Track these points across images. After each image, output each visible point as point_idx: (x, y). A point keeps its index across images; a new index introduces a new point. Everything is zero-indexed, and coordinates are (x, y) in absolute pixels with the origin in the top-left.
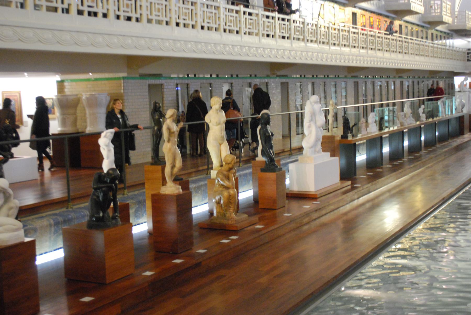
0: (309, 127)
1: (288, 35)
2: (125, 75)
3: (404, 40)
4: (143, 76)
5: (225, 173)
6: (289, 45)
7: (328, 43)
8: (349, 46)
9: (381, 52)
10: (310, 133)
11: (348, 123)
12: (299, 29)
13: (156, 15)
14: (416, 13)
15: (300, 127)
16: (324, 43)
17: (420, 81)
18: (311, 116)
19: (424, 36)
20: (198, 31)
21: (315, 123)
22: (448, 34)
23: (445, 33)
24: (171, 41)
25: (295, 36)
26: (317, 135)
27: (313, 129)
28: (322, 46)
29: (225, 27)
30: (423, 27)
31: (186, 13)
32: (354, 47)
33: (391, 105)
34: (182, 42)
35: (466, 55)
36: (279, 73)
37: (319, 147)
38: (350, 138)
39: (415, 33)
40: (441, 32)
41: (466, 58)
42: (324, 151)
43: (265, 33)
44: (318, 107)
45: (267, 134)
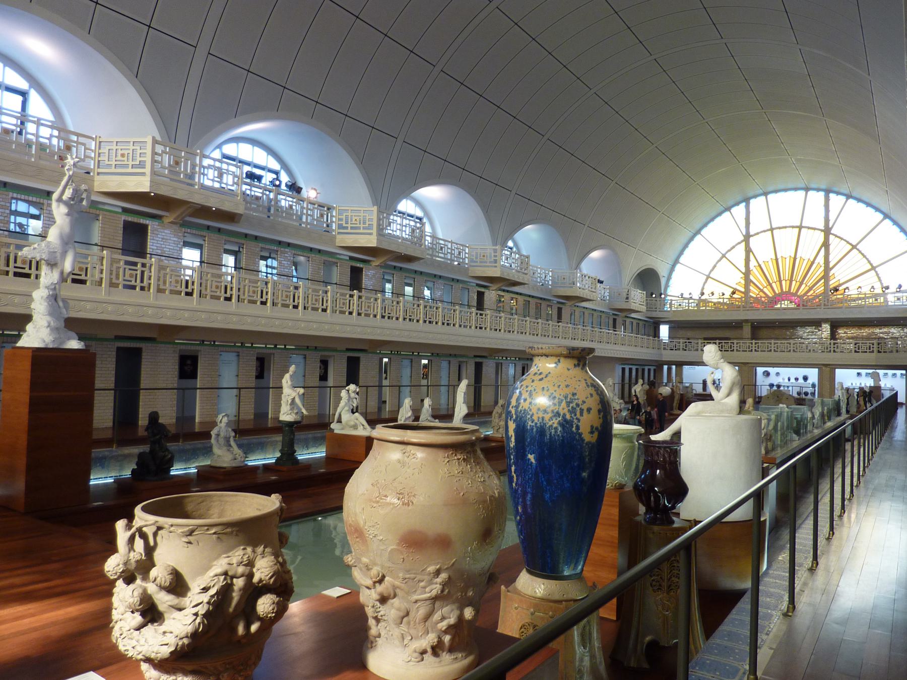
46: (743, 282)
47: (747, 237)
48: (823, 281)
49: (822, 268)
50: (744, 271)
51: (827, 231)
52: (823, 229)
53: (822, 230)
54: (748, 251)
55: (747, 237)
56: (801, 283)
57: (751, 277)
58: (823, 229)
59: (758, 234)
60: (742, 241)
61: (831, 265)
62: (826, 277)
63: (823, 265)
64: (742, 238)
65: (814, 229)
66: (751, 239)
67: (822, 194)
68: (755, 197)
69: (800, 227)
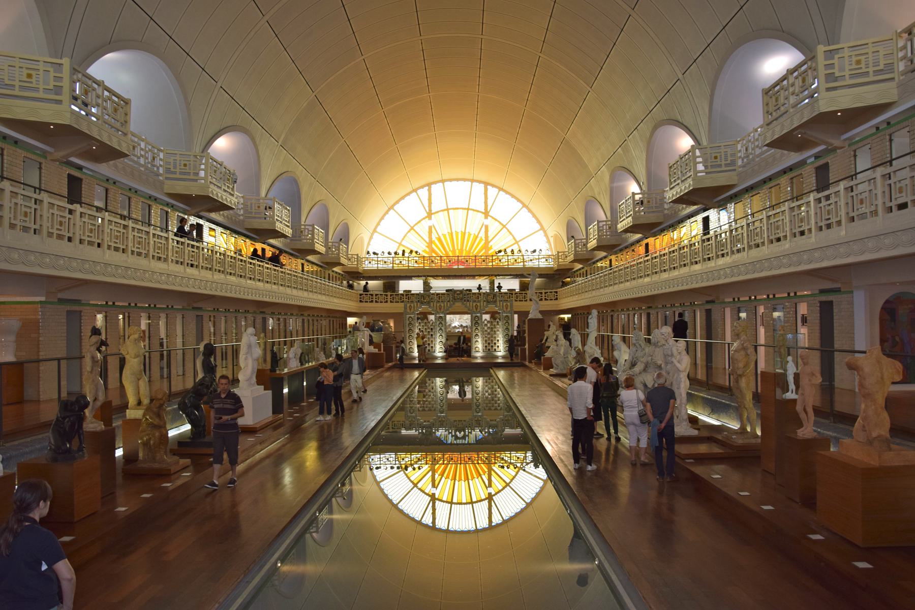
0: (246, 359)
1: (210, 266)
2: (43, 299)
3: (305, 277)
4: (61, 301)
5: (155, 410)
6: (211, 277)
8: (262, 281)
10: (246, 366)
11: (276, 357)
12: (220, 260)
13: (88, 236)
14: (319, 253)
15: (224, 361)
16: (241, 276)
17: (315, 319)
18: (248, 348)
19: (323, 276)
20: (128, 256)
21: (252, 356)
24: (102, 265)
25: (217, 268)
26: (253, 366)
29: (154, 254)
30: (321, 266)
31: (117, 236)
32: (267, 282)
33: (306, 341)
34: (113, 266)
36: (195, 305)
37: (254, 379)
38: (278, 372)
39: (319, 273)
42: (259, 383)
43: (190, 262)
44: (254, 339)
48: (484, 251)
62: (486, 246)
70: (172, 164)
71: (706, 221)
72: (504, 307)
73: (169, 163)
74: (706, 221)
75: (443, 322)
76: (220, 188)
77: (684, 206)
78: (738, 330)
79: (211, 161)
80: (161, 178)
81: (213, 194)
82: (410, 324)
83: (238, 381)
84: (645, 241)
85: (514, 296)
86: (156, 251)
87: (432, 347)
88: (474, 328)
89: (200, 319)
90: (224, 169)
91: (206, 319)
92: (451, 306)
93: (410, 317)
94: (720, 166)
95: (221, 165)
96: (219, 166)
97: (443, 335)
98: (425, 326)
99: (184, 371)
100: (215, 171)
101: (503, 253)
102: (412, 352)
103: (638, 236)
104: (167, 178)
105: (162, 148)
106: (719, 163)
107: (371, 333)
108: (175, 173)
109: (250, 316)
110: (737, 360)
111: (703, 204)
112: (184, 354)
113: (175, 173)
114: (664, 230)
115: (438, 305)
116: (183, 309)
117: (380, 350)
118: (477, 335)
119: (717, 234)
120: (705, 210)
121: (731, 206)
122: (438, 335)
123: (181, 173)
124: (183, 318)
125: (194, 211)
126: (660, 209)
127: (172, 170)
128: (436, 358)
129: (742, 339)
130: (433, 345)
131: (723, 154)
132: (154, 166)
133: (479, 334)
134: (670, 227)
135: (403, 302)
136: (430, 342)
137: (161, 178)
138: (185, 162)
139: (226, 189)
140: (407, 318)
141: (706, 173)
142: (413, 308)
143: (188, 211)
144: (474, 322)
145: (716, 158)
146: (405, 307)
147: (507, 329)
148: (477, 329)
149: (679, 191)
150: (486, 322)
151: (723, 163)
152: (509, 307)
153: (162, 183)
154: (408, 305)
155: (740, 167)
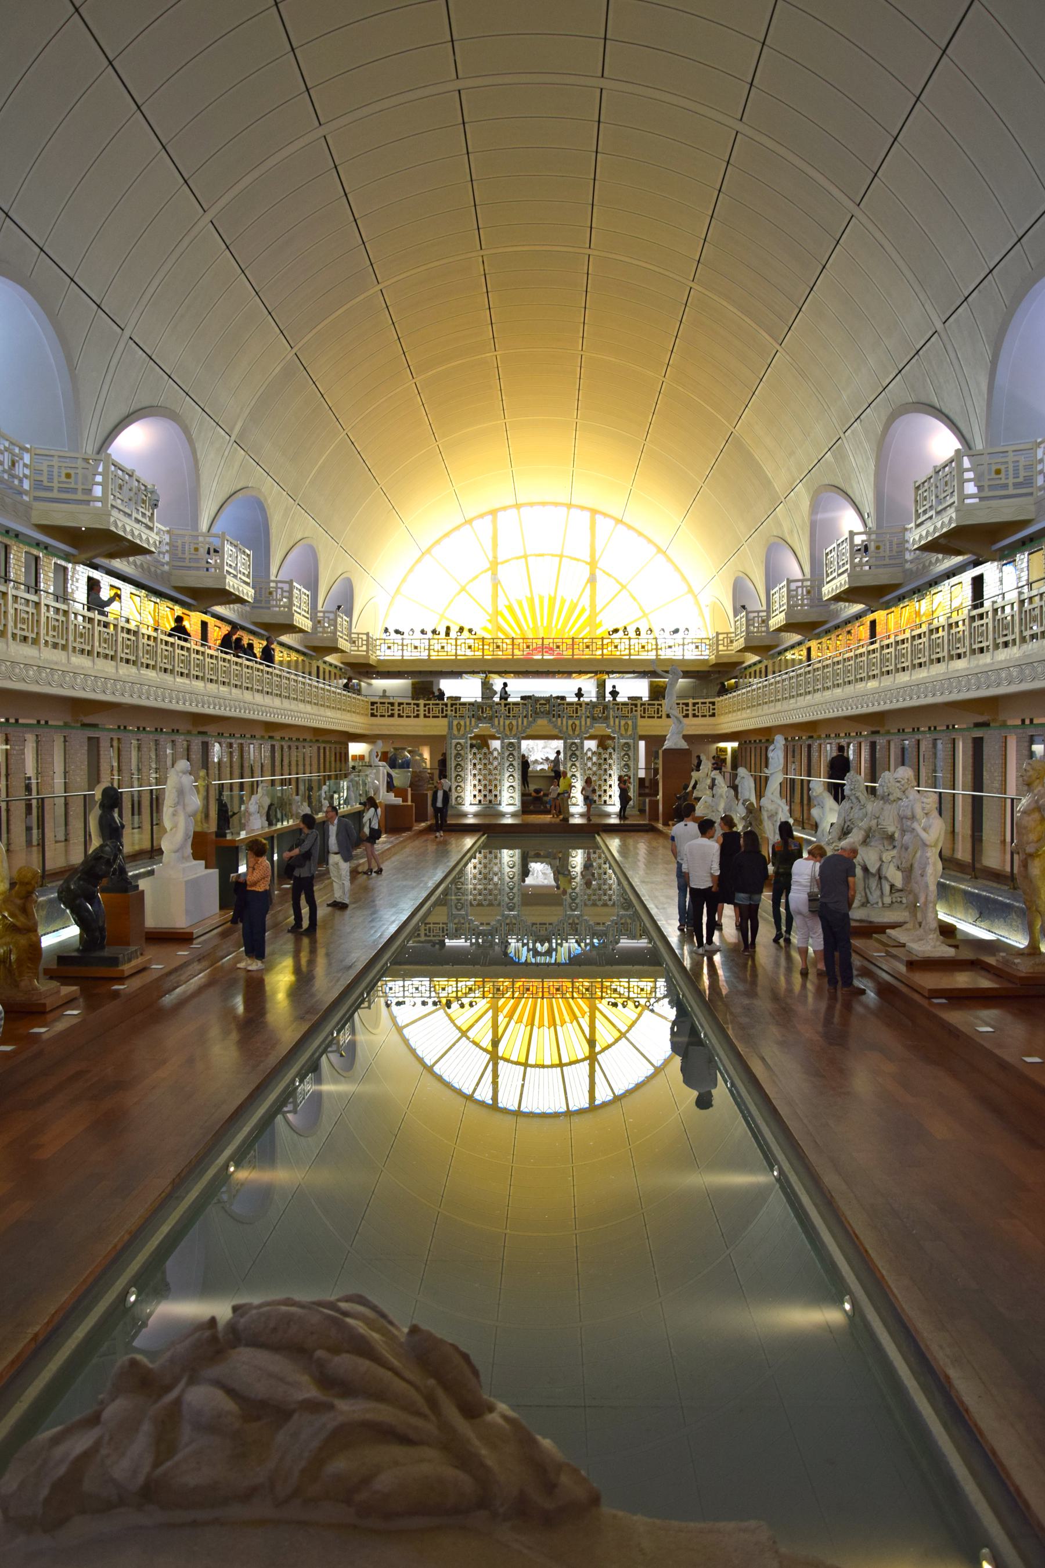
0: (174, 815)
7: (172, 671)
9: (249, 692)
10: (175, 826)
11: (227, 811)
15: (136, 817)
17: (300, 745)
18: (178, 797)
21: (184, 808)
22: (341, 669)
23: (336, 667)
27: (181, 820)
28: (162, 675)
35: (370, 707)
38: (229, 837)
40: (331, 665)
41: (370, 711)
42: (196, 856)
44: (188, 780)
45: (114, 826)
46: (489, 626)
47: (495, 564)
48: (588, 629)
49: (587, 613)
50: (490, 611)
51: (593, 564)
52: (589, 560)
53: (587, 563)
54: (496, 581)
55: (495, 564)
56: (563, 631)
57: (500, 619)
58: (589, 560)
59: (508, 561)
60: (486, 571)
61: (598, 609)
62: (592, 621)
63: (588, 609)
64: (488, 565)
65: (578, 560)
66: (499, 566)
67: (587, 514)
68: (504, 509)
69: (561, 556)
70: (45, 473)
71: (978, 583)
72: (622, 728)
73: (40, 472)
74: (978, 583)
75: (515, 753)
76: (130, 516)
77: (940, 556)
78: (1030, 777)
79: (113, 468)
80: (26, 498)
81: (116, 526)
82: (458, 755)
83: (160, 852)
84: (871, 617)
85: (639, 708)
86: (19, 626)
87: (496, 796)
88: (569, 764)
89: (94, 744)
90: (136, 484)
91: (104, 744)
92: (529, 724)
93: (458, 743)
94: (1005, 486)
95: (130, 476)
96: (127, 477)
97: (516, 775)
98: (485, 758)
99: (67, 834)
100: (120, 487)
101: (620, 634)
102: (460, 804)
103: (858, 607)
104: (36, 499)
105: (28, 446)
106: (1003, 481)
107: (391, 771)
108: (50, 489)
109: (180, 739)
110: (1025, 828)
111: (974, 554)
112: (66, 804)
113: (50, 489)
114: (904, 598)
115: (507, 722)
116: (66, 725)
117: (405, 800)
118: (574, 775)
119: (996, 606)
120: (976, 564)
121: (1022, 558)
122: (507, 774)
123: (61, 490)
124: (65, 741)
125: (84, 557)
126: (897, 561)
127: (45, 483)
128: (503, 815)
129: (1036, 791)
130: (498, 793)
131: (1011, 466)
132: (14, 476)
133: (578, 774)
134: (914, 593)
135: (446, 716)
136: (492, 788)
137: (26, 498)
138: (69, 471)
139: (140, 517)
140: (453, 745)
141: (981, 499)
142: (462, 728)
143: (73, 555)
144: (569, 753)
145: (998, 472)
146: (450, 726)
147: (625, 765)
148: (573, 765)
149: (931, 529)
150: (589, 754)
151: (1011, 481)
152: (630, 728)
153: (28, 507)
154: (455, 722)
155: (1040, 489)
